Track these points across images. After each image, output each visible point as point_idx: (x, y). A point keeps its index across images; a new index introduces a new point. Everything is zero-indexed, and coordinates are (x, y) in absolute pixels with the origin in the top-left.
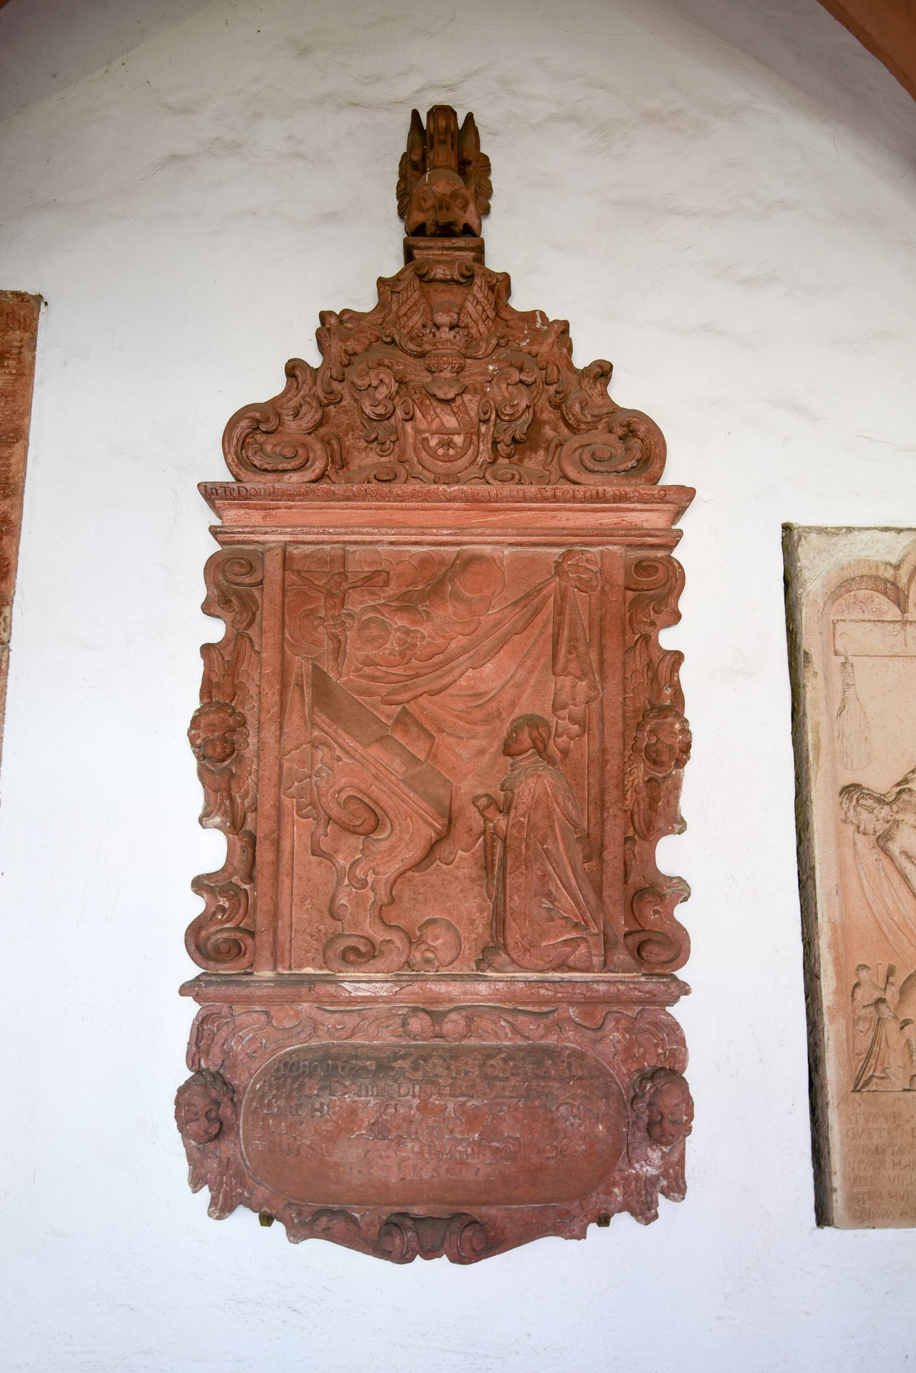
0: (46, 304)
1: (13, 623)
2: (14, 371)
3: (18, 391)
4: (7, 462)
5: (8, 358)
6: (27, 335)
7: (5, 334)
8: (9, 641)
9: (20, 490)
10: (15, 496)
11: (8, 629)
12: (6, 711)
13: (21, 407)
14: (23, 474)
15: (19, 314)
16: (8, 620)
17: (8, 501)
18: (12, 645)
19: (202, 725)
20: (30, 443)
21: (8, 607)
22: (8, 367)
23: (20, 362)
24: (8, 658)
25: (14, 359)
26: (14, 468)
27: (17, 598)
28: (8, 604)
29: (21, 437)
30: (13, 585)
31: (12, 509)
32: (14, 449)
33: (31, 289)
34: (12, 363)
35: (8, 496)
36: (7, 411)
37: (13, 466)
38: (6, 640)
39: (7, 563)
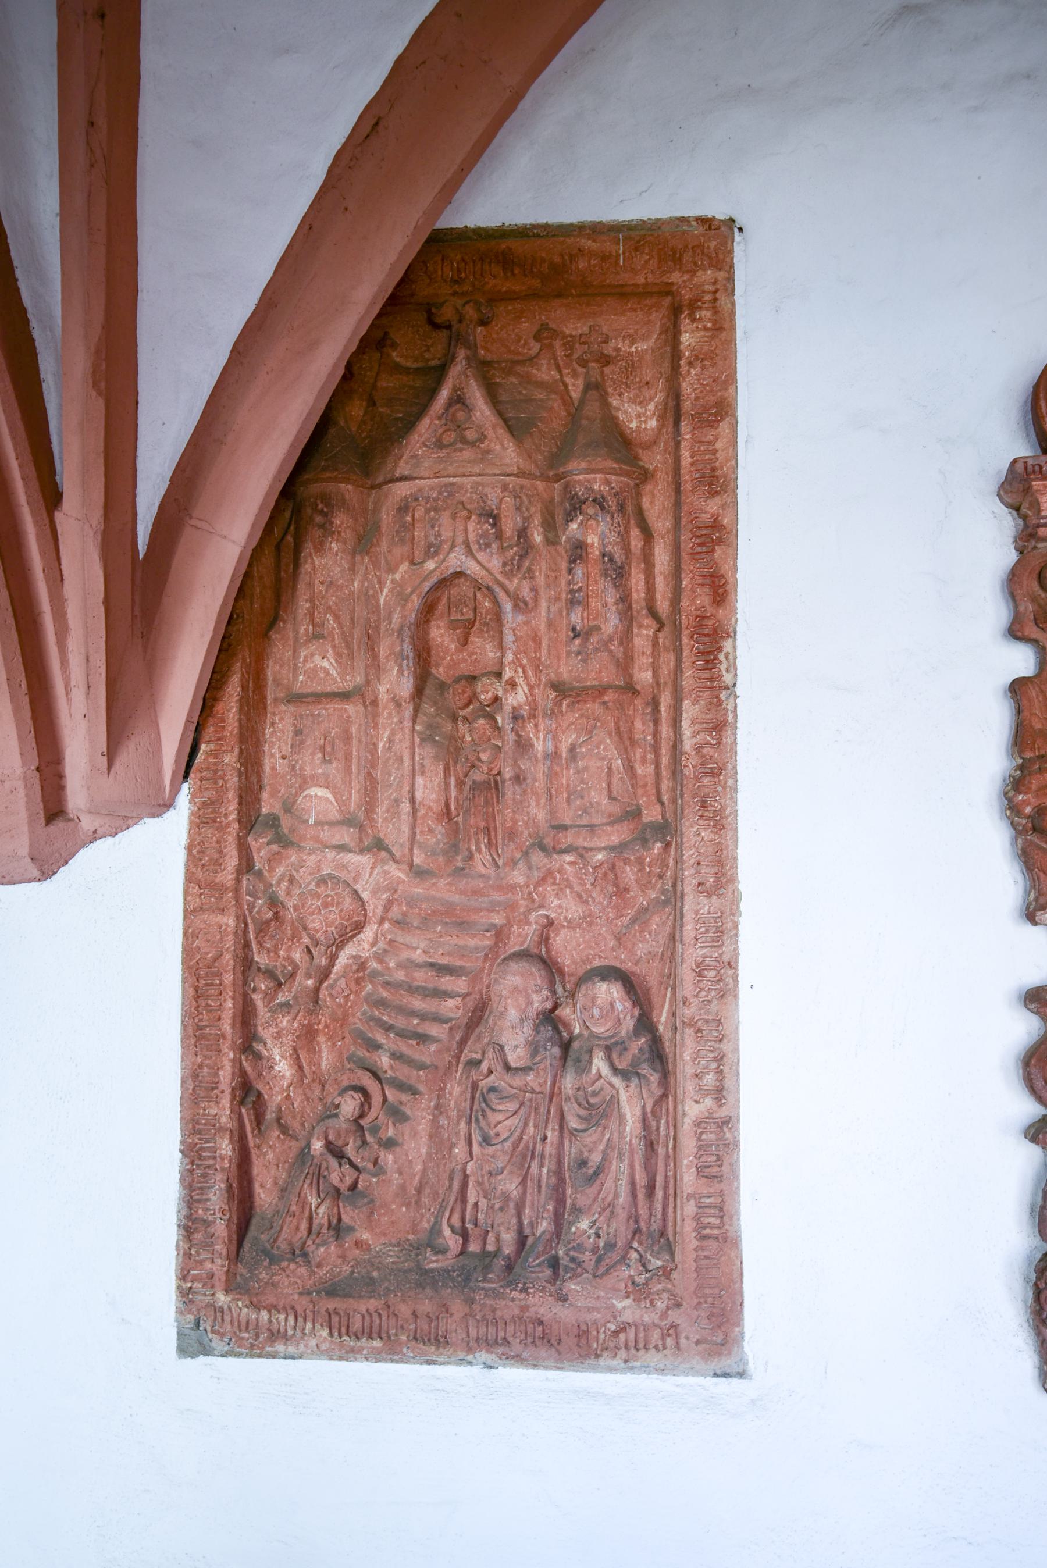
0: (741, 230)
1: (738, 661)
2: (709, 325)
3: (717, 352)
4: (711, 448)
5: (700, 308)
6: (722, 275)
7: (692, 276)
8: (734, 685)
9: (732, 485)
10: (726, 492)
11: (732, 669)
12: (739, 777)
13: (723, 373)
14: (733, 462)
15: (709, 247)
16: (731, 657)
17: (717, 499)
18: (738, 690)
19: (1034, 787)
20: (739, 419)
21: (730, 640)
22: (700, 319)
23: (716, 312)
24: (735, 707)
25: (707, 309)
26: (721, 456)
27: (741, 628)
28: (729, 636)
29: (727, 413)
30: (733, 611)
31: (723, 509)
32: (720, 429)
33: (719, 211)
34: (706, 314)
35: (717, 493)
36: (704, 379)
37: (720, 452)
38: (730, 684)
39: (723, 581)
